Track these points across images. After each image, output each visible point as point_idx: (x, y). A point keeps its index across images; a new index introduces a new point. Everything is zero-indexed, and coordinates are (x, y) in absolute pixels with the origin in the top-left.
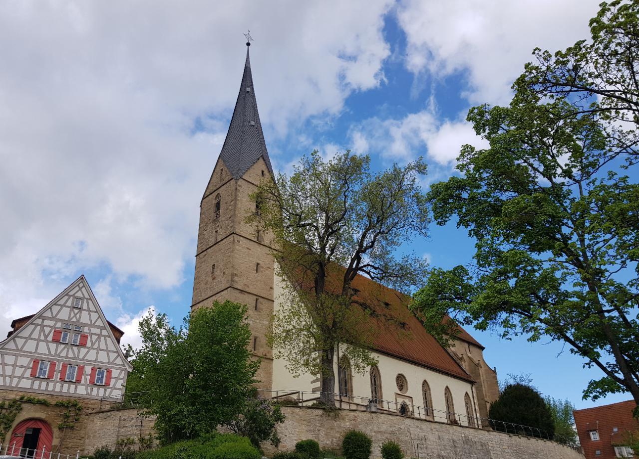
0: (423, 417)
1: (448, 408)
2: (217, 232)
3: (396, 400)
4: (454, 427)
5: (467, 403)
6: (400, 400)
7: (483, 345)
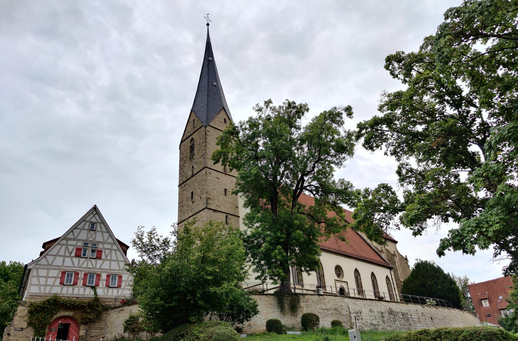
0: (357, 296)
1: (374, 289)
2: (193, 167)
3: (336, 285)
4: (381, 302)
5: (387, 284)
6: (339, 285)
7: (396, 239)
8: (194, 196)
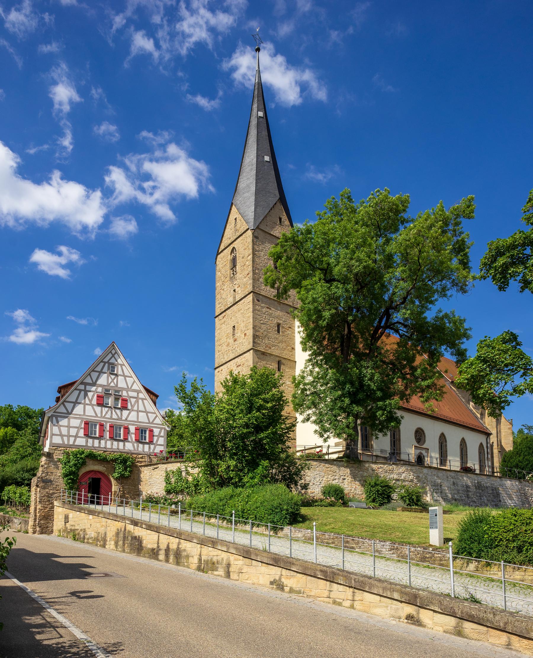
2: (234, 291)
5: (480, 453)
8: (236, 331)
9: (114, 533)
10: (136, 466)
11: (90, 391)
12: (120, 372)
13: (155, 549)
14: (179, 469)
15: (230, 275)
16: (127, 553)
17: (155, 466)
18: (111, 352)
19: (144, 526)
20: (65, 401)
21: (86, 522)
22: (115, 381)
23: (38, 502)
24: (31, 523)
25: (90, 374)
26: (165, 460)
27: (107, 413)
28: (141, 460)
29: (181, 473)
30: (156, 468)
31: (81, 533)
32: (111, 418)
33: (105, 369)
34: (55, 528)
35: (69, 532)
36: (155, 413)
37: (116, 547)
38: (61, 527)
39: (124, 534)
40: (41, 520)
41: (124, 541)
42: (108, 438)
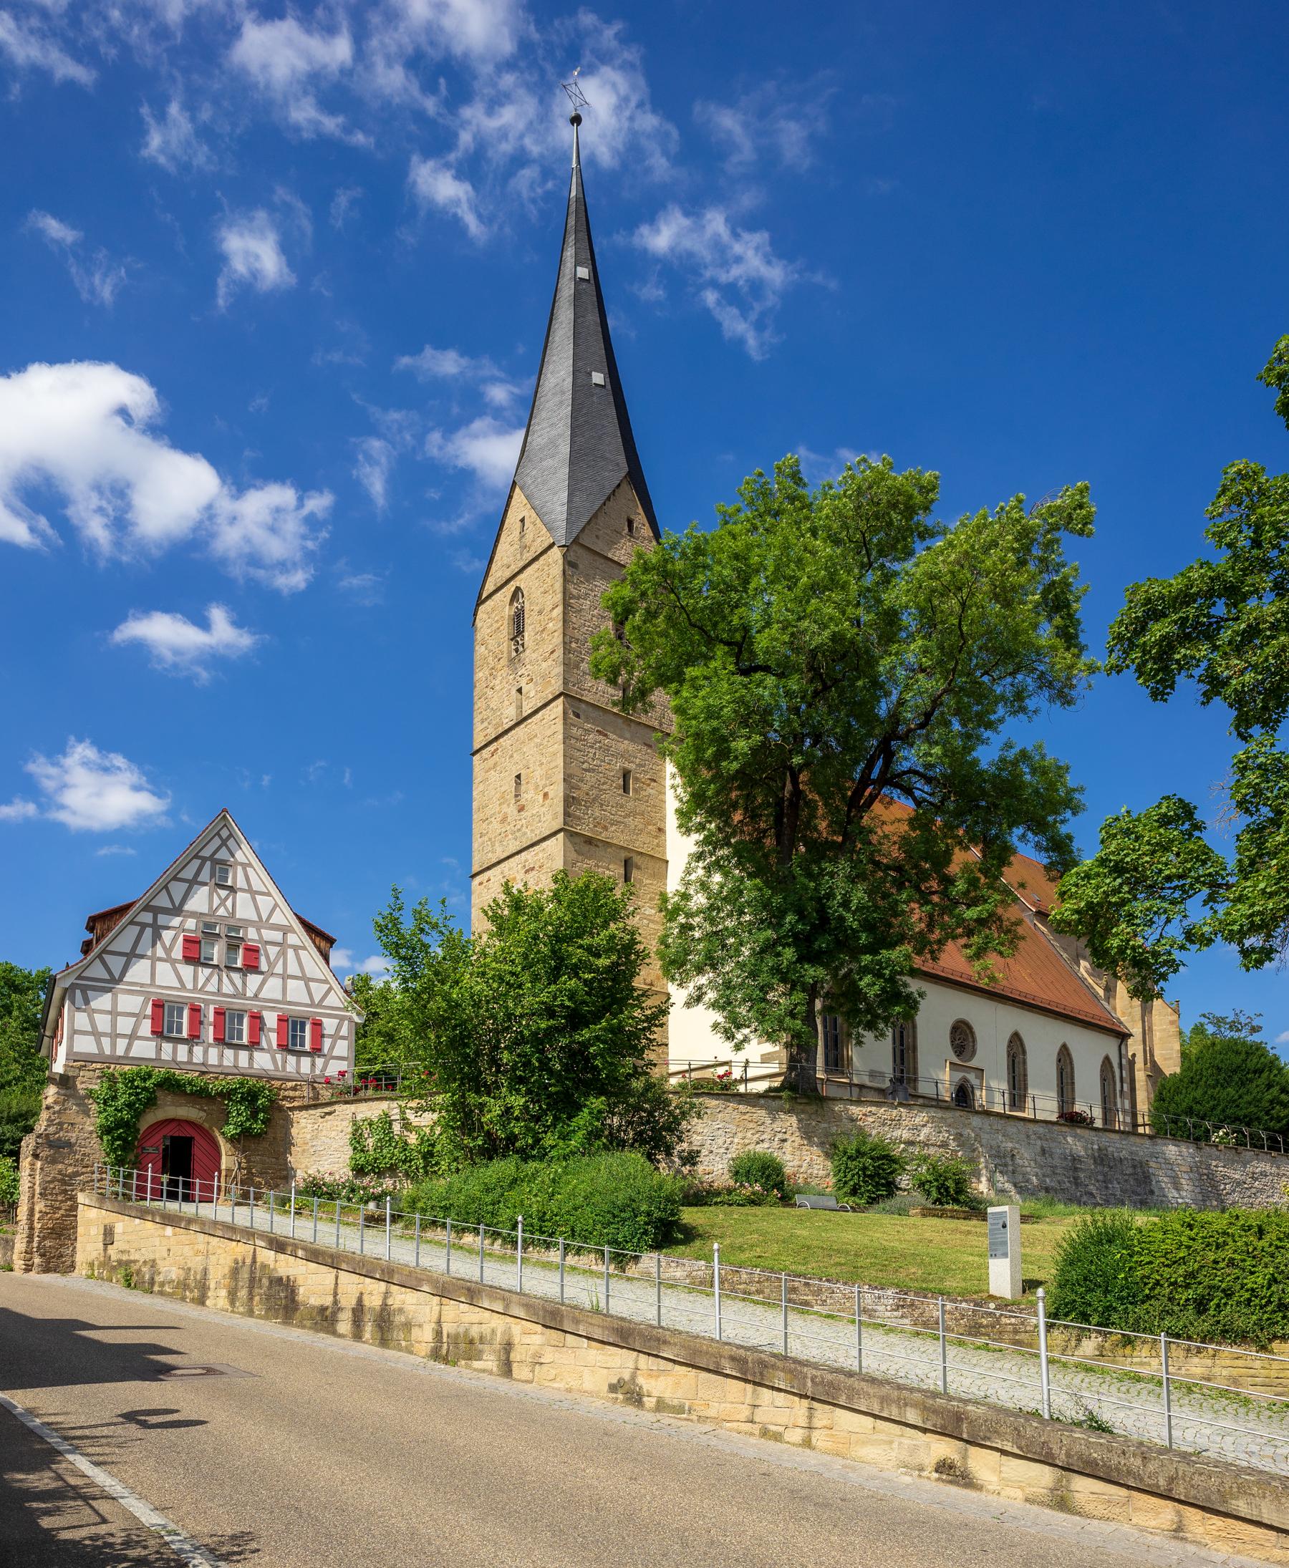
2: (520, 691)
5: (1103, 1080)
8: (523, 788)
9: (226, 1270)
10: (280, 1109)
11: (168, 928)
12: (241, 883)
13: (327, 1308)
14: (387, 1115)
15: (509, 653)
16: (260, 1317)
17: (328, 1109)
18: (218, 834)
19: (300, 1253)
20: (104, 951)
21: (157, 1243)
22: (229, 903)
23: (37, 1196)
24: (20, 1245)
25: (166, 887)
26: (352, 1094)
27: (208, 980)
28: (291, 1093)
29: (391, 1125)
30: (330, 1114)
31: (144, 1269)
32: (219, 992)
33: (205, 875)
34: (79, 1258)
35: (114, 1268)
36: (326, 981)
37: (232, 1303)
38: (95, 1254)
39: (252, 1272)
40: (44, 1238)
41: (251, 1289)
42: (211, 1040)
